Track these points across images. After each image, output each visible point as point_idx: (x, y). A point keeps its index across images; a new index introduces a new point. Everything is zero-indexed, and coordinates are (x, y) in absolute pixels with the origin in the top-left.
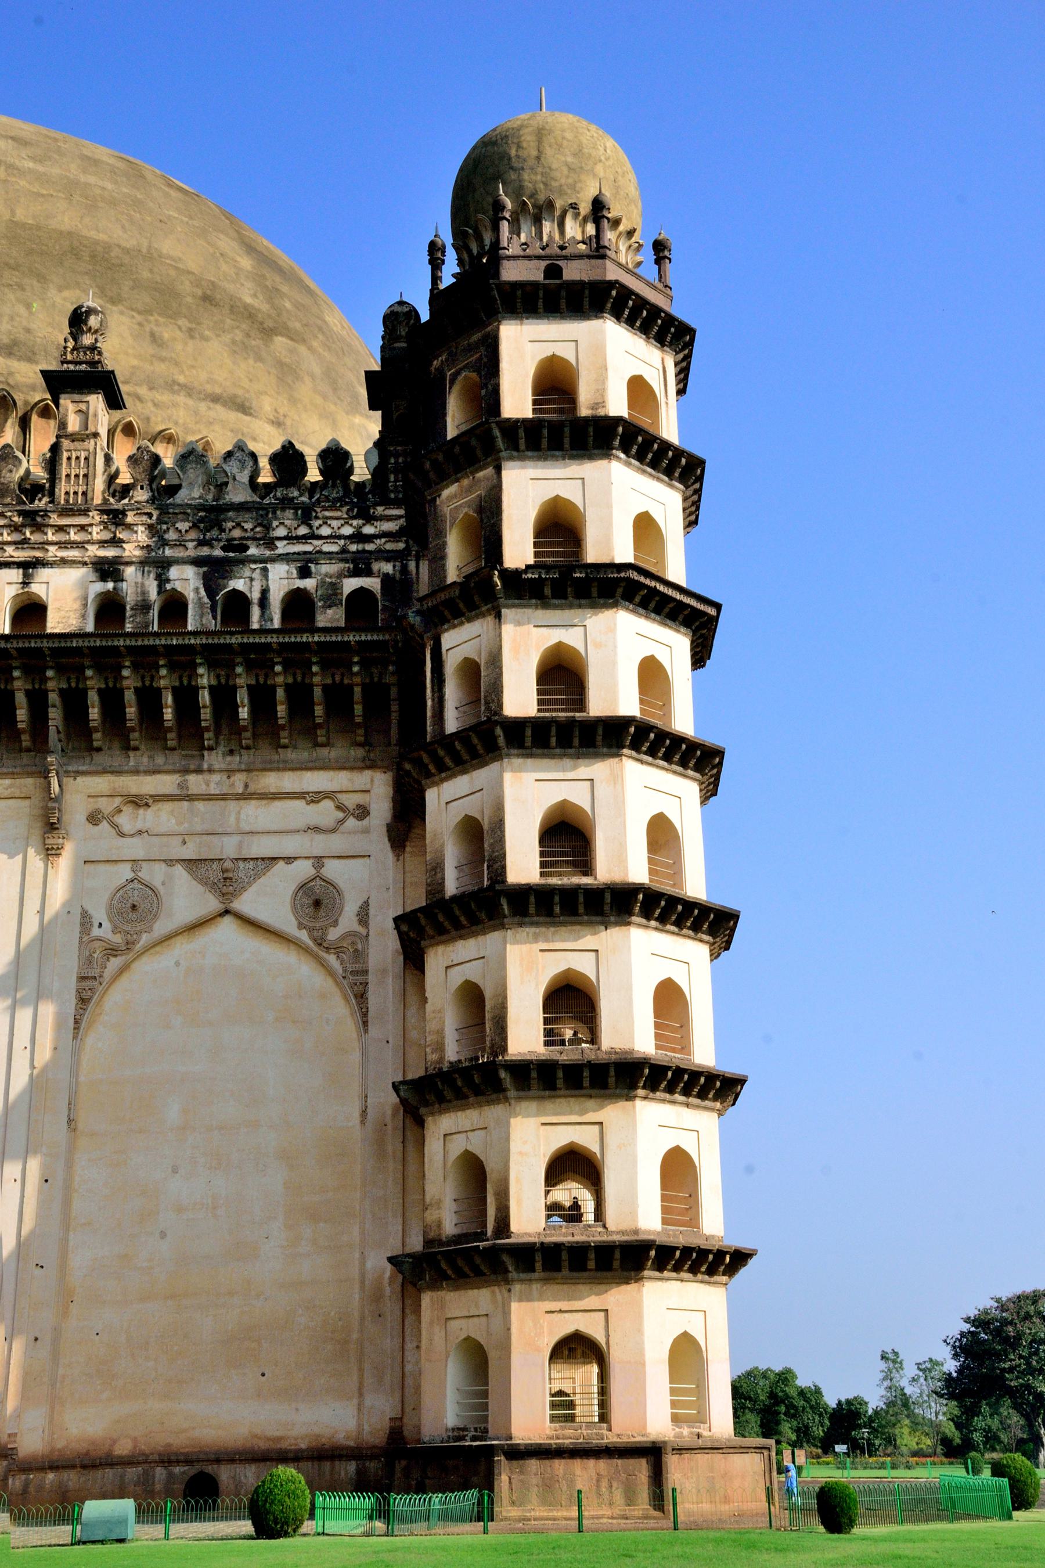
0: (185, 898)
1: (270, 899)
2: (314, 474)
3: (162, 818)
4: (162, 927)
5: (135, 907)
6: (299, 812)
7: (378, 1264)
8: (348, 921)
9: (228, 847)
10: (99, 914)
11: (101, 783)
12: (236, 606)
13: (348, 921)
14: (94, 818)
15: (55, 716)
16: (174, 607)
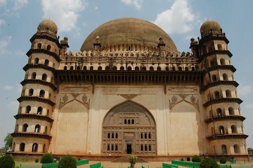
0: (179, 99)
1: (188, 99)
2: (185, 55)
3: (176, 90)
4: (177, 102)
5: (174, 99)
6: (190, 90)
7: (204, 137)
8: (196, 101)
9: (183, 93)
10: (171, 100)
11: (169, 86)
12: (180, 68)
13: (196, 101)
14: (169, 90)
15: (165, 79)
16: (174, 68)
